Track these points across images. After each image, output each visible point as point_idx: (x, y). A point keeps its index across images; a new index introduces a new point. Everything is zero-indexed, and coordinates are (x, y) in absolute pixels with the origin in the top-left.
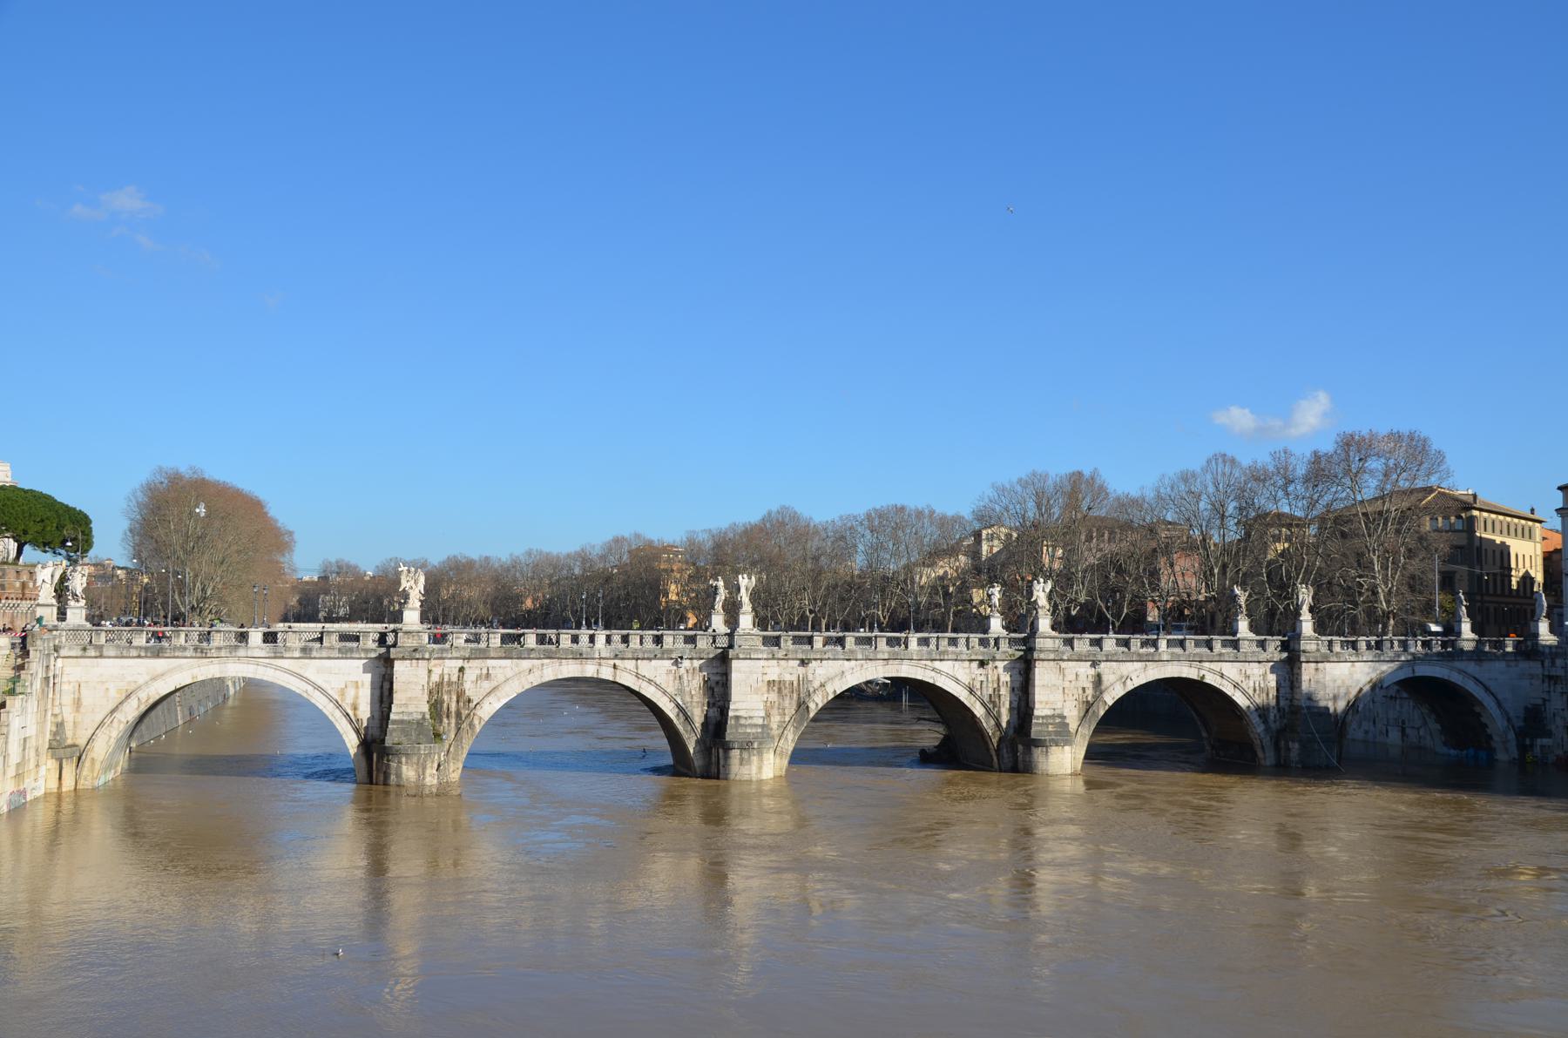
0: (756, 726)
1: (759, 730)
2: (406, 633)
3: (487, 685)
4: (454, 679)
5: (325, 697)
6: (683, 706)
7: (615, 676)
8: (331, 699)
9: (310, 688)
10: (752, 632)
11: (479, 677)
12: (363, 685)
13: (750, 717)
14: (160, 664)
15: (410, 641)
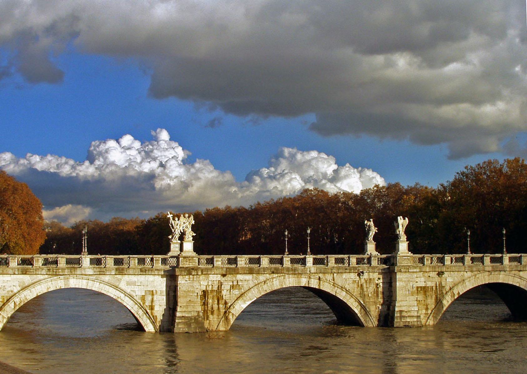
0: (413, 316)
1: (415, 320)
2: (185, 257)
3: (237, 292)
4: (215, 288)
5: (132, 302)
6: (364, 305)
7: (319, 285)
8: (136, 303)
9: (122, 296)
10: (408, 254)
11: (233, 287)
12: (156, 293)
13: (409, 311)
14: (27, 279)
15: (188, 263)
